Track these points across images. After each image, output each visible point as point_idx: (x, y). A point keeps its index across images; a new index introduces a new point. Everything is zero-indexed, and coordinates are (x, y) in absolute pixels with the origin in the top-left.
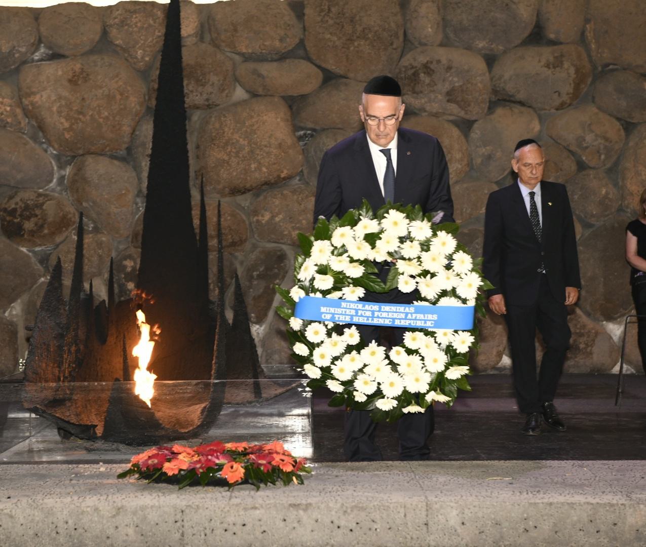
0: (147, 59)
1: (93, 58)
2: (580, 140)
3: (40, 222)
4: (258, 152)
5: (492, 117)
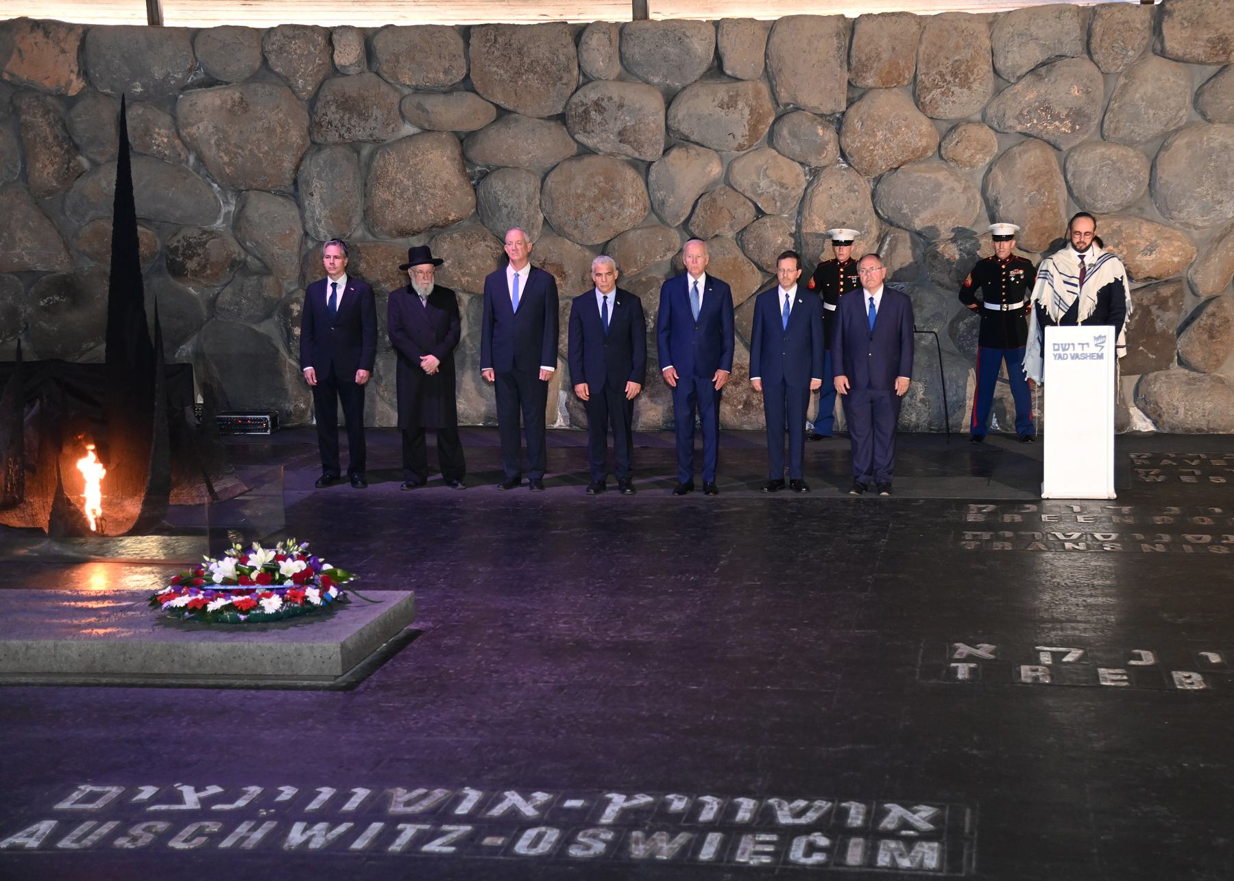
1: (253, 86)
2: (755, 186)
3: (203, 262)
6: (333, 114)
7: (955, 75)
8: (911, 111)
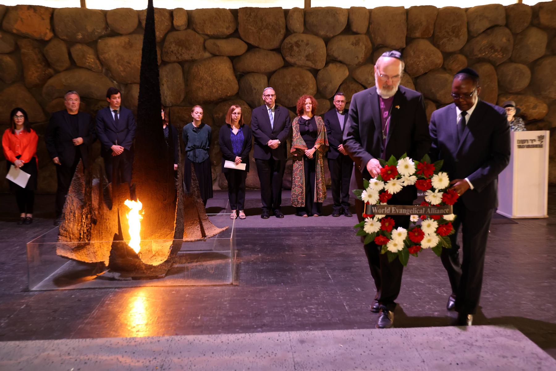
0: (161, 36)
1: (134, 35)
4: (216, 83)
5: (327, 68)
6: (173, 47)
7: (453, 33)
8: (433, 48)
